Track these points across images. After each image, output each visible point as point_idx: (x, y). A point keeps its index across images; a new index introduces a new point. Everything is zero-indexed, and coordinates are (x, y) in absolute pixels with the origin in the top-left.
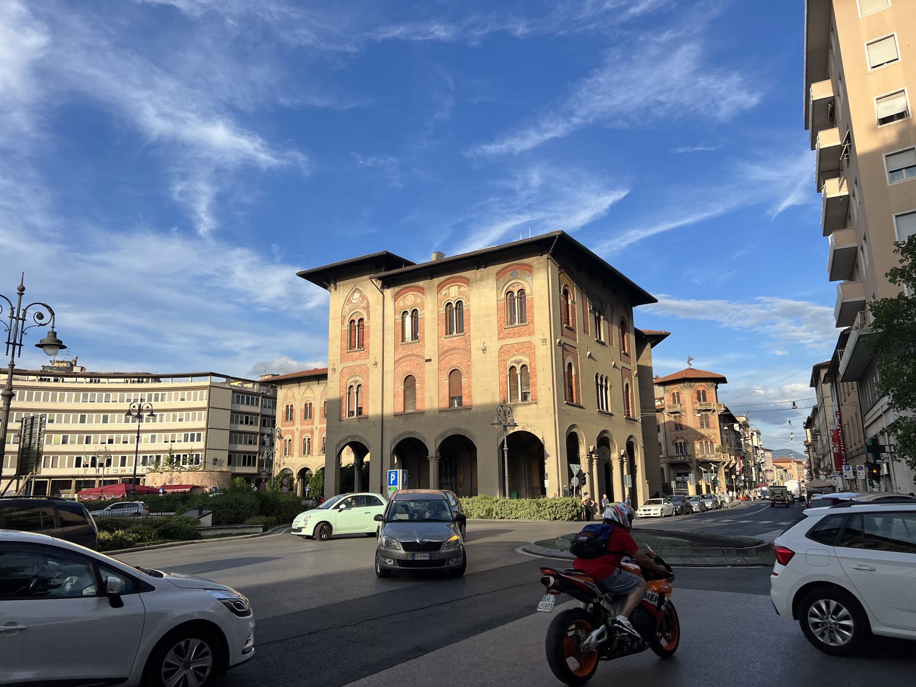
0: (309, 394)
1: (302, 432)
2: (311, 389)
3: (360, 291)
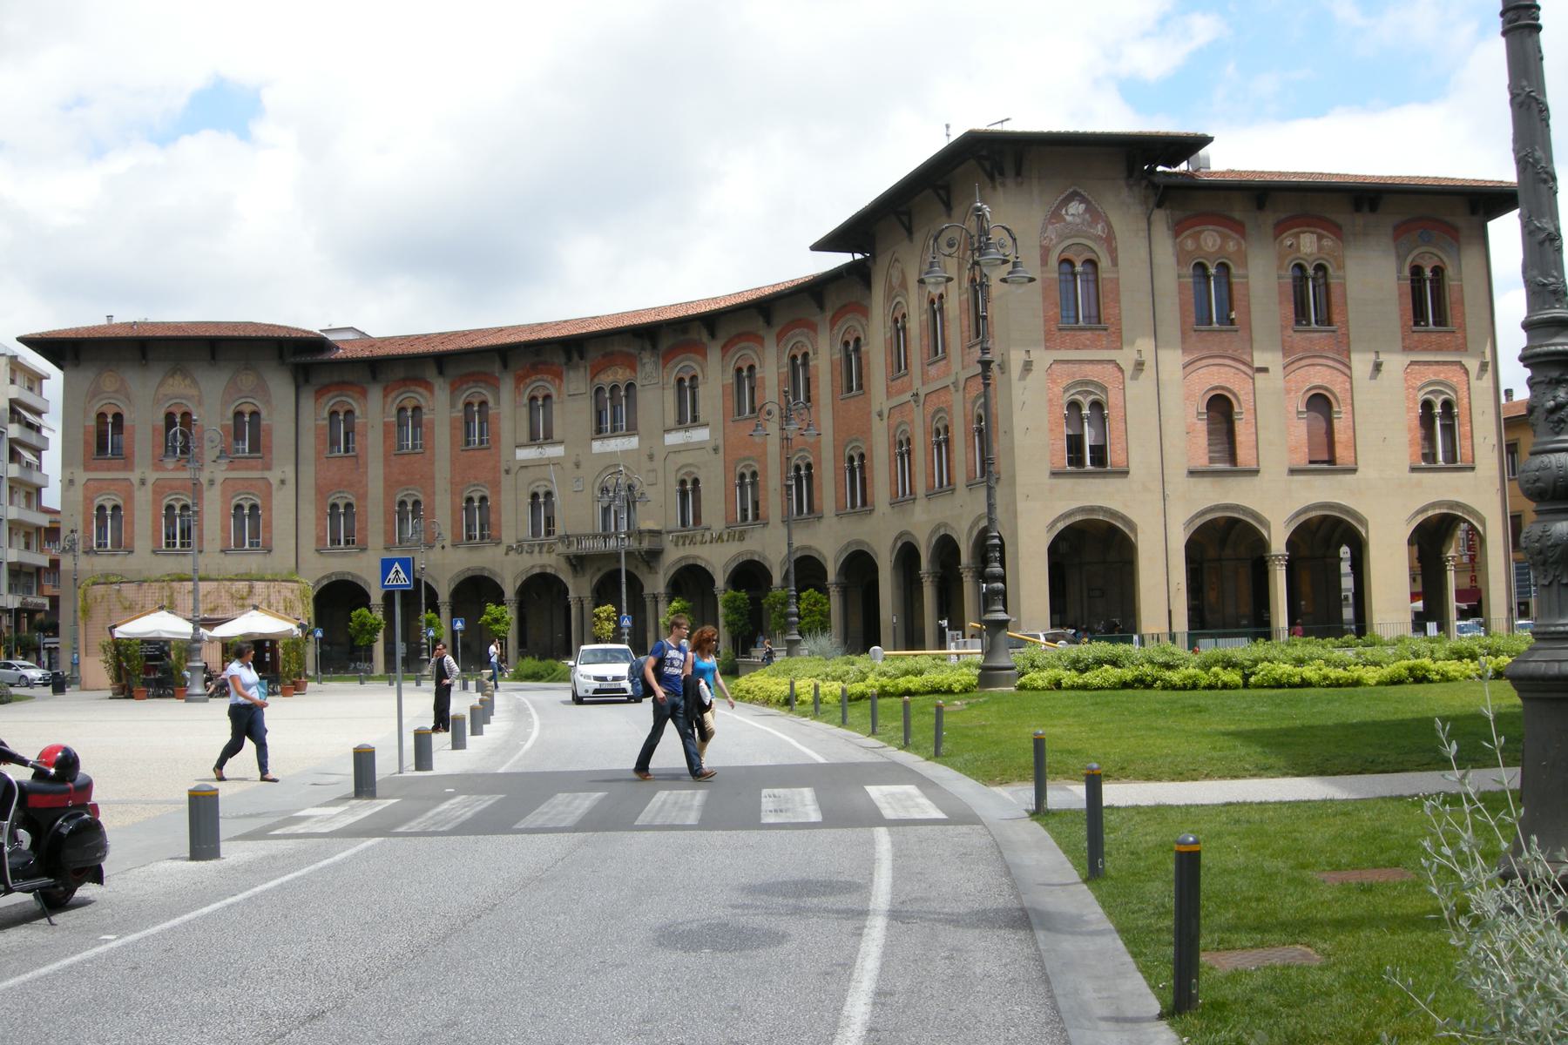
1: (159, 489)
3: (1083, 200)
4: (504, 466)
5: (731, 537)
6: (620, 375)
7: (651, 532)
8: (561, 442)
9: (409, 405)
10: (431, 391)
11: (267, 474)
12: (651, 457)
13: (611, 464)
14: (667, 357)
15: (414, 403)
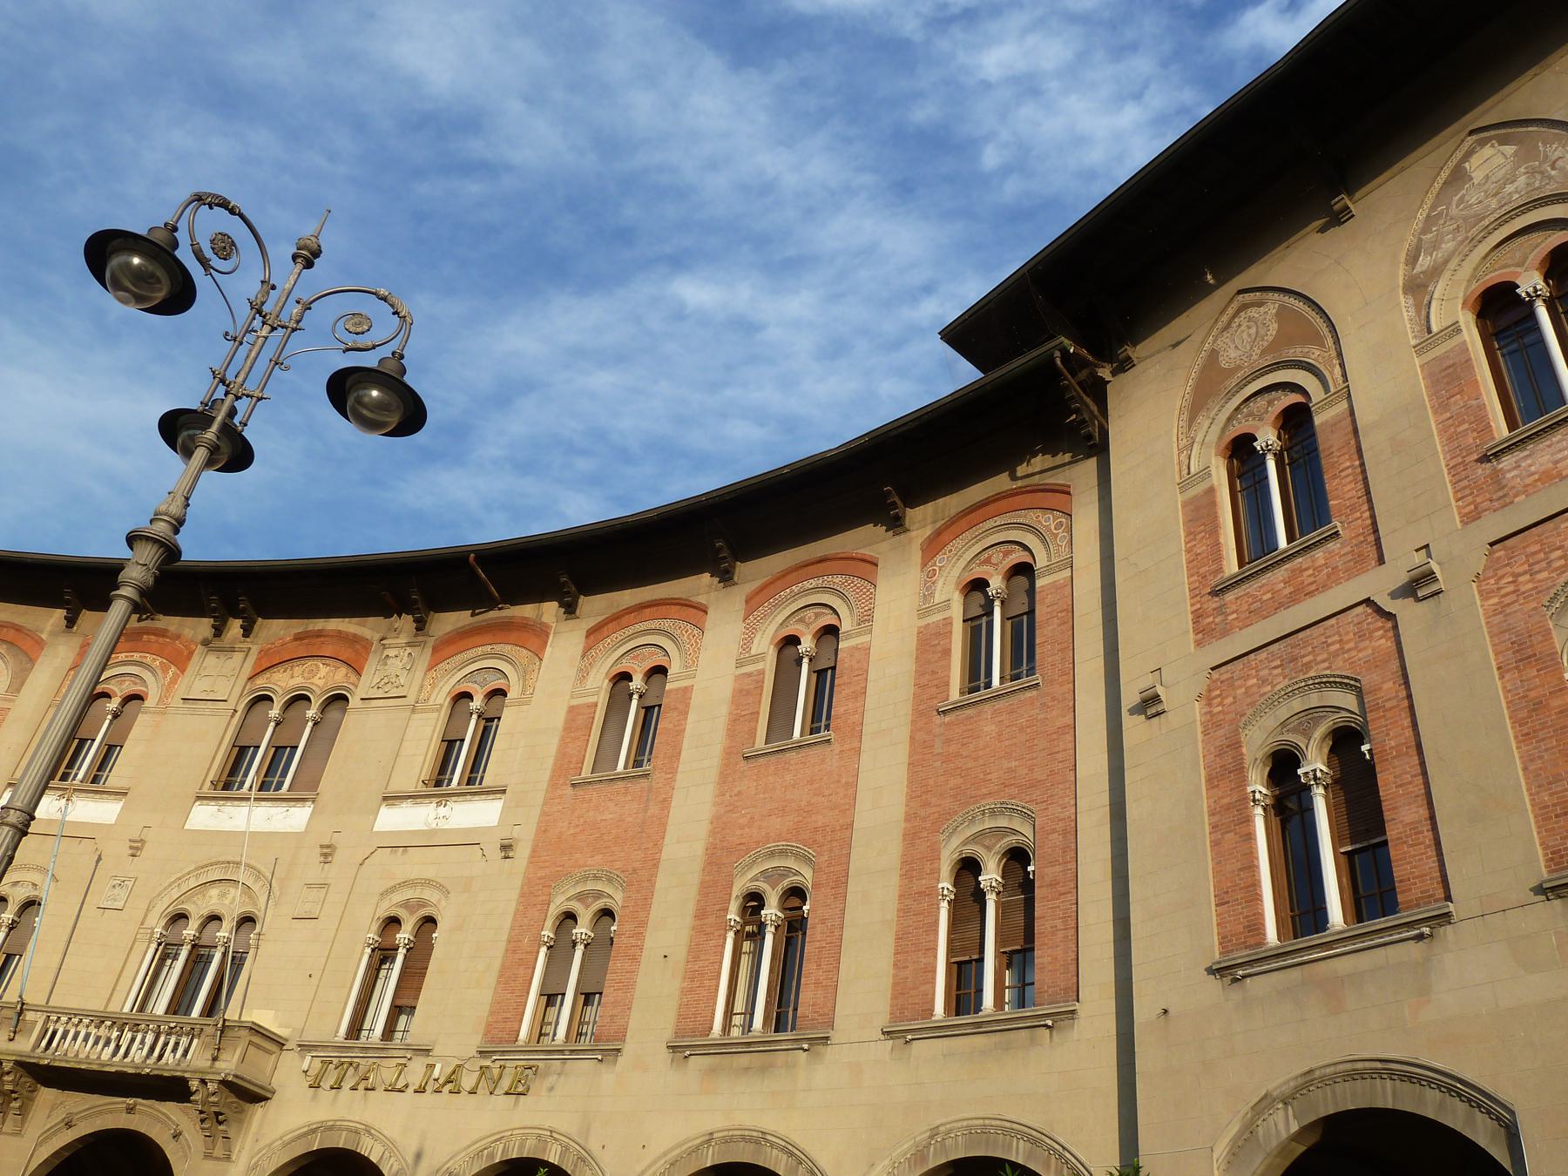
5: (489, 1081)
6: (321, 677)
7: (256, 1030)
12: (327, 853)
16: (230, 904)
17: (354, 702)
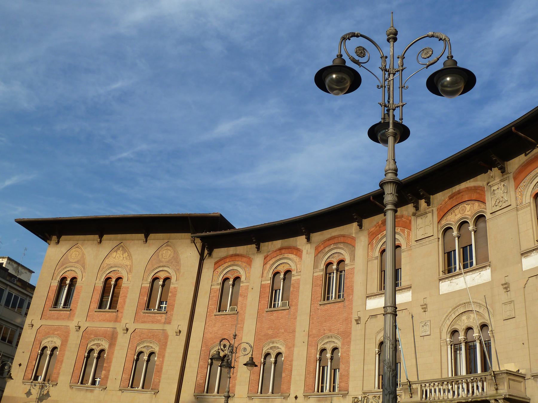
0: (118, 259)
1: (87, 335)
2: (125, 250)
4: (355, 316)
6: (468, 211)
7: (509, 373)
8: (409, 288)
9: (282, 269)
10: (300, 256)
11: (167, 327)
12: (506, 287)
13: (463, 304)
14: (519, 176)
15: (286, 268)
16: (474, 321)
17: (488, 216)
